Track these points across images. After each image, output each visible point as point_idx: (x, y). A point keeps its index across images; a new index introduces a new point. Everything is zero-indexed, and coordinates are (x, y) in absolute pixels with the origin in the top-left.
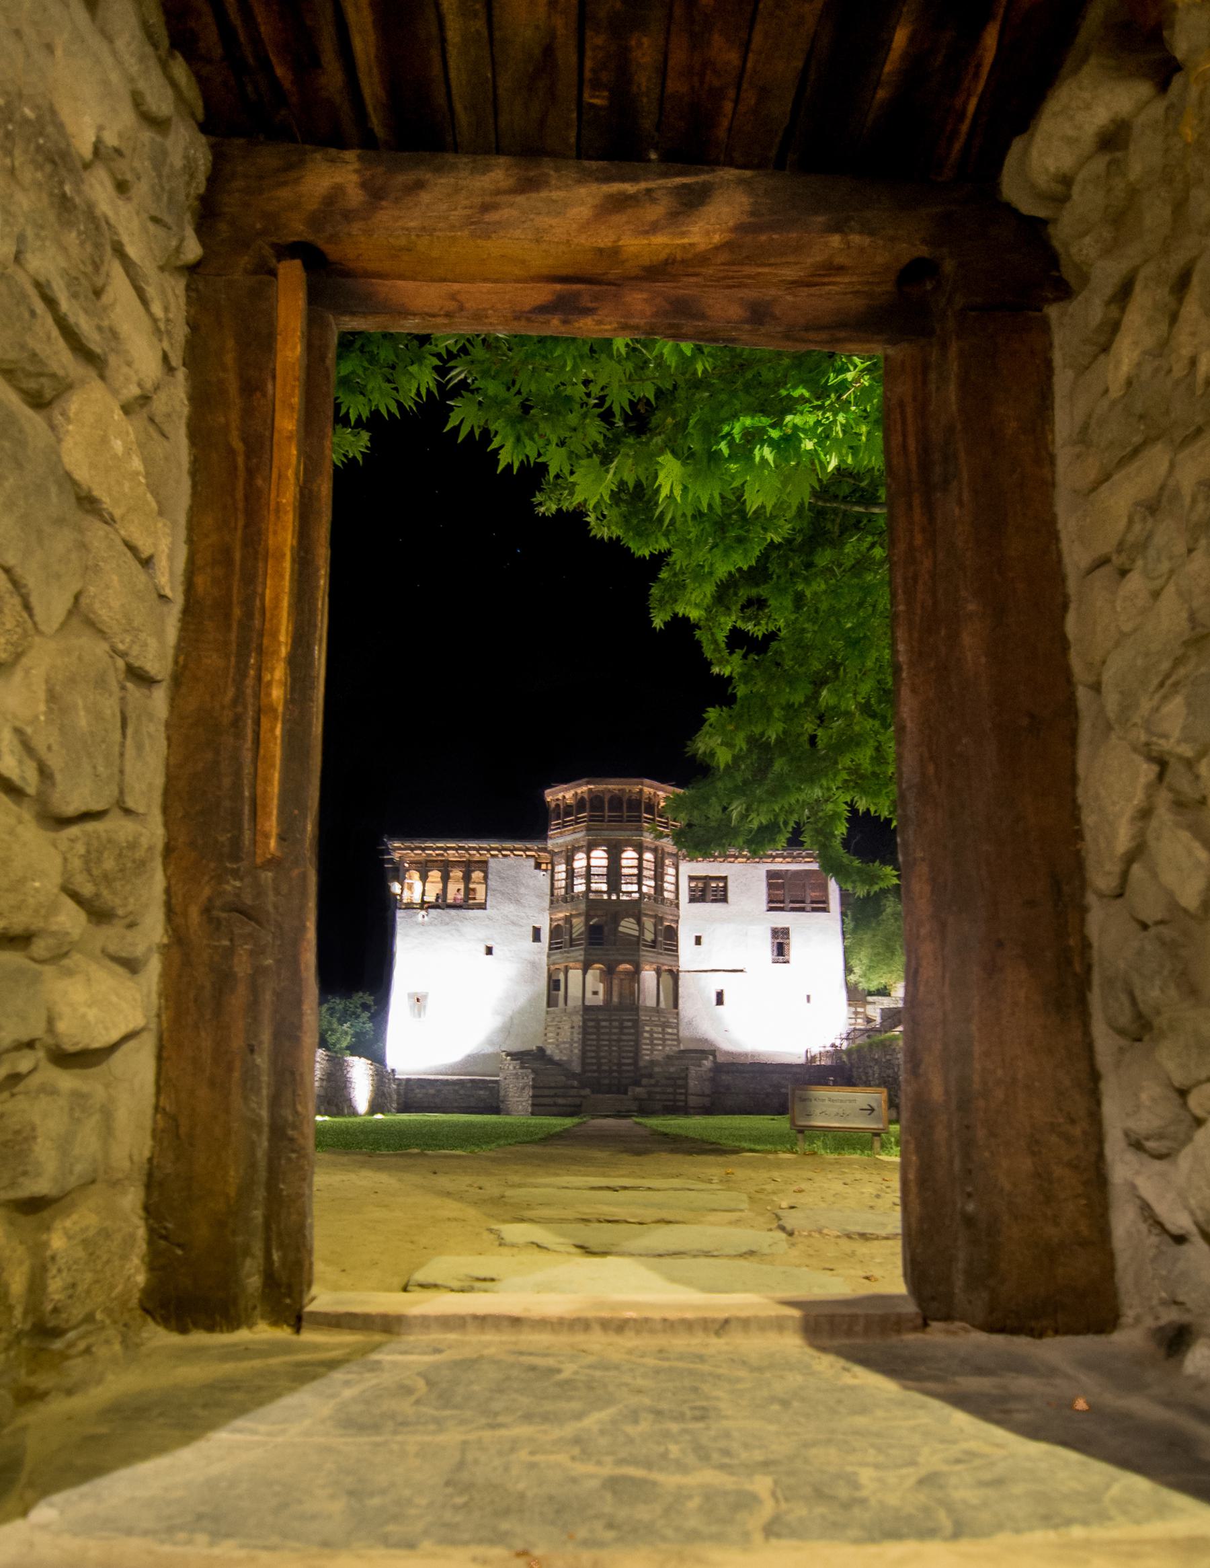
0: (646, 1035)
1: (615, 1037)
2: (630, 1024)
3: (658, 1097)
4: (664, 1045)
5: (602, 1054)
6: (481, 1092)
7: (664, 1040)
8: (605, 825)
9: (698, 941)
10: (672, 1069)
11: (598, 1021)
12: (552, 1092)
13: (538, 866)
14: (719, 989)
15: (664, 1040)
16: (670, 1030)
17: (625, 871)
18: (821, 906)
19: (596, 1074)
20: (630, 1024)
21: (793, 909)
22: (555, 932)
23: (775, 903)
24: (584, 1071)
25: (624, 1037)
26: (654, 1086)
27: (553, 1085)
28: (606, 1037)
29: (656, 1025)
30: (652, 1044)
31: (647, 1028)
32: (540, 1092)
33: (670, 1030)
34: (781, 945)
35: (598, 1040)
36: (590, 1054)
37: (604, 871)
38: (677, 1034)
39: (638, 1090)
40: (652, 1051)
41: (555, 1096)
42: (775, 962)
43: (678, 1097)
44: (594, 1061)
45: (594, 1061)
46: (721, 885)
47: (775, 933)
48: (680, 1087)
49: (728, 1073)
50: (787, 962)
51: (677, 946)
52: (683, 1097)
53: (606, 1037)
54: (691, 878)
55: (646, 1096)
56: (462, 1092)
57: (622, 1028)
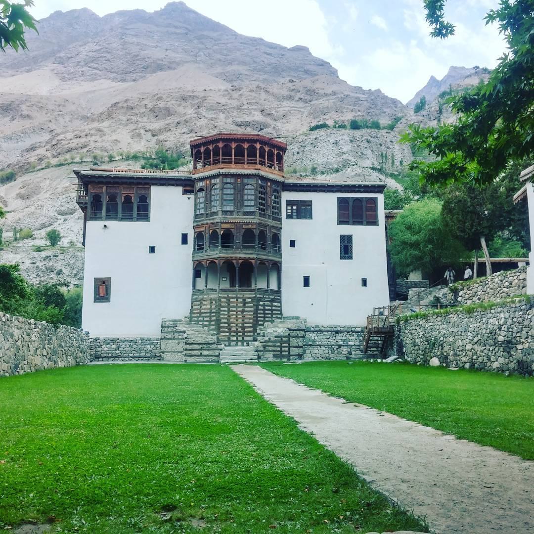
0: (260, 307)
1: (239, 309)
2: (250, 300)
3: (270, 349)
4: (272, 314)
5: (231, 320)
6: (149, 346)
7: (272, 310)
8: (233, 166)
9: (292, 244)
10: (279, 331)
11: (228, 299)
12: (199, 347)
13: (185, 192)
16: (276, 304)
17: (246, 197)
18: (375, 223)
19: (228, 334)
20: (250, 300)
21: (353, 224)
22: (199, 237)
23: (343, 220)
24: (219, 332)
25: (246, 309)
26: (266, 341)
27: (199, 342)
28: (235, 309)
30: (264, 314)
31: (261, 303)
32: (188, 347)
33: (276, 304)
34: (346, 248)
35: (229, 311)
36: (223, 320)
37: (232, 197)
38: (281, 307)
39: (256, 343)
40: (264, 317)
41: (201, 349)
42: (342, 258)
43: (283, 349)
44: (226, 325)
45: (226, 325)
47: (343, 238)
48: (285, 342)
49: (313, 332)
50: (351, 258)
51: (280, 247)
52: (286, 349)
54: (289, 203)
55: (262, 349)
56: (135, 346)
57: (245, 303)
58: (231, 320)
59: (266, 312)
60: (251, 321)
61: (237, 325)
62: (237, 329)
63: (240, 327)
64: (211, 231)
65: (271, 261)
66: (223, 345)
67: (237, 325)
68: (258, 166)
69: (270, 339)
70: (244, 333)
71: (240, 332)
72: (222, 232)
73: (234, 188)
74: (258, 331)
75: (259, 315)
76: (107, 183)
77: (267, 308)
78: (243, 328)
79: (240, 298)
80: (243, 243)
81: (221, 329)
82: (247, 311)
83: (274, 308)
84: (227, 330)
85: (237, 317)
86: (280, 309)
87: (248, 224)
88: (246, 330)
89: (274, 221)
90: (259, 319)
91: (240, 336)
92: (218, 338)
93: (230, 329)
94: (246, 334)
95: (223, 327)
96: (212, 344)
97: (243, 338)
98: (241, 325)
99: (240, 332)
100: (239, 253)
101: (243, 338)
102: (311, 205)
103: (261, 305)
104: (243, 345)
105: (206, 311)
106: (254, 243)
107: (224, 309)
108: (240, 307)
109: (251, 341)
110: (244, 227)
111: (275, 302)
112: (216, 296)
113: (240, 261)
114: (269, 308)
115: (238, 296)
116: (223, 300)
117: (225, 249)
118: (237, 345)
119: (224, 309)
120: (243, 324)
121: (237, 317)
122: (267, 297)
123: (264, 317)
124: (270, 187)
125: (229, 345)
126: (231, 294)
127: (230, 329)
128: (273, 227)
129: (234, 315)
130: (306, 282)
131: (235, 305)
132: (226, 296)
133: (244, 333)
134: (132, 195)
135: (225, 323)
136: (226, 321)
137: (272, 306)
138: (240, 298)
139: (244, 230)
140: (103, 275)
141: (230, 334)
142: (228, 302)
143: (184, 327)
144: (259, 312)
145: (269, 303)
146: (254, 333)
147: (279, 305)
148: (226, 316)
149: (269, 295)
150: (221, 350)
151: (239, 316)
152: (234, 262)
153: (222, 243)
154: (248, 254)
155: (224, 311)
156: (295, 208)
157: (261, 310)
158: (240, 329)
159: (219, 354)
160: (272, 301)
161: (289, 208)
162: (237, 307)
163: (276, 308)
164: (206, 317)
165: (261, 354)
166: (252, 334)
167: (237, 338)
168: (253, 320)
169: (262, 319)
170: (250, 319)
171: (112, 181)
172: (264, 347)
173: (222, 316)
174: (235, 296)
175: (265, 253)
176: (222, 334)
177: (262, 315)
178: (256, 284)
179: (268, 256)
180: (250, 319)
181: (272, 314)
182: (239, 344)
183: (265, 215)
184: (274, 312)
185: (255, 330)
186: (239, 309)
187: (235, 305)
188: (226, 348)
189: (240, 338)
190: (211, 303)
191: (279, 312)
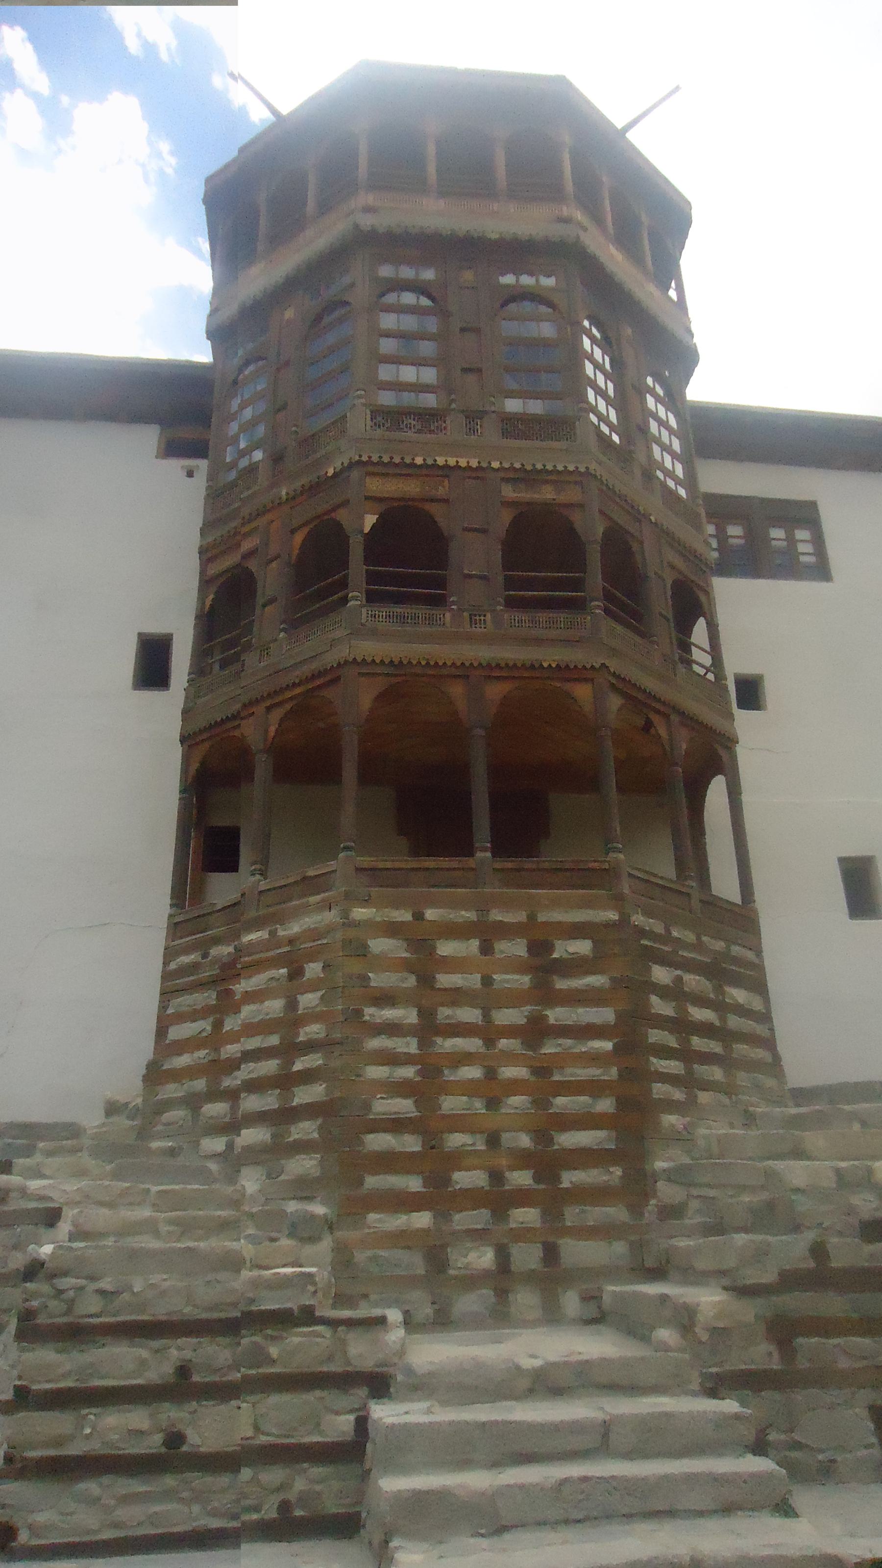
2: (582, 947)
5: (450, 1104)
16: (738, 995)
19: (422, 1220)
20: (582, 947)
22: (227, 605)
25: (556, 1015)
26: (790, 1281)
28: (469, 1015)
30: (686, 1055)
31: (661, 974)
33: (738, 995)
35: (429, 1029)
38: (766, 1017)
40: (689, 1082)
44: (411, 1143)
45: (411, 1143)
46: (802, 534)
53: (469, 1015)
57: (543, 965)
58: (450, 1104)
59: (697, 1042)
60: (606, 1105)
61: (493, 1141)
62: (496, 1177)
63: (524, 1159)
64: (299, 538)
66: (395, 1335)
67: (493, 1141)
69: (818, 1251)
70: (553, 1201)
71: (522, 1198)
72: (370, 520)
73: (441, 310)
74: (668, 1193)
78: (547, 1164)
80: (510, 583)
81: (372, 1182)
82: (563, 1031)
84: (414, 1184)
85: (491, 1074)
88: (569, 1179)
90: (659, 1090)
91: (523, 1234)
92: (343, 1260)
93: (438, 1181)
94: (572, 1215)
95: (388, 1162)
96: (283, 1319)
97: (551, 1253)
98: (525, 1141)
99: (522, 1198)
101: (551, 1253)
103: (665, 992)
104: (552, 1316)
105: (253, 1043)
106: (577, 585)
107: (389, 1014)
108: (514, 999)
109: (610, 1273)
110: (508, 492)
111: (738, 981)
112: (331, 917)
113: (495, 691)
115: (496, 915)
116: (379, 945)
117: (383, 611)
118: (500, 1317)
119: (389, 1014)
120: (542, 1136)
121: (491, 1074)
122: (690, 937)
123: (689, 1082)
125: (442, 1321)
126: (434, 904)
127: (438, 1181)
129: (466, 1058)
131: (474, 981)
132: (404, 916)
133: (553, 1201)
135: (396, 1125)
136: (405, 1106)
137: (721, 1007)
141: (442, 1216)
142: (424, 964)
143: (81, 1173)
146: (636, 1209)
148: (408, 1072)
150: (379, 1384)
151: (509, 1072)
152: (457, 690)
153: (372, 578)
154: (539, 642)
155: (393, 1029)
156: (735, 531)
157: (661, 1022)
158: (522, 1178)
159: (362, 1423)
162: (488, 997)
164: (254, 1086)
166: (617, 1213)
167: (503, 1254)
168: (622, 1103)
170: (594, 1088)
172: (783, 1331)
173: (376, 1072)
174: (470, 915)
176: (380, 1221)
180: (594, 1088)
182: (525, 1299)
184: (741, 1049)
185: (637, 1187)
186: (507, 1016)
187: (474, 981)
188: (433, 1353)
189: (527, 1257)
190: (296, 973)
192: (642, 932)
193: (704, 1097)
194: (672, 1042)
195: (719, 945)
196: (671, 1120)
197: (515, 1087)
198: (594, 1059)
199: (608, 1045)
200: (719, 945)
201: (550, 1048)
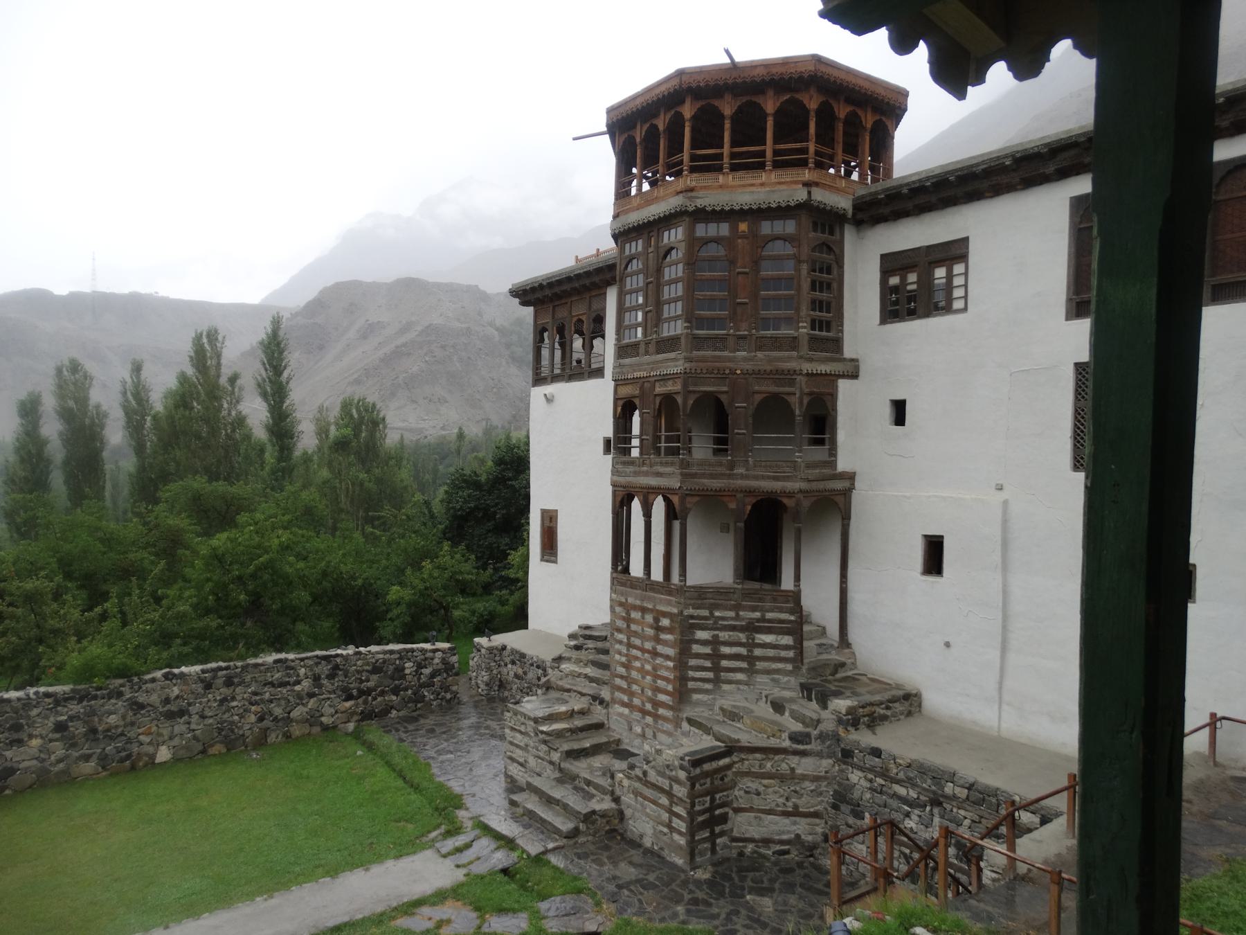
0: (696, 648)
2: (665, 622)
4: (751, 671)
5: (634, 674)
7: (751, 659)
9: (899, 411)
14: (933, 531)
15: (751, 659)
16: (769, 638)
19: (626, 711)
20: (665, 622)
25: (660, 648)
29: (733, 628)
30: (716, 669)
31: (702, 635)
40: (717, 681)
46: (958, 268)
54: (892, 264)
59: (724, 663)
65: (749, 492)
68: (689, 180)
75: (691, 673)
76: (551, 300)
77: (726, 650)
79: (651, 611)
82: (661, 655)
83: (758, 652)
86: (791, 654)
87: (665, 379)
89: (760, 354)
90: (691, 685)
91: (648, 725)
100: (646, 474)
102: (963, 258)
103: (704, 643)
110: (659, 389)
111: (769, 631)
114: (743, 651)
122: (732, 614)
124: (753, 235)
128: (759, 375)
130: (933, 555)
134: (584, 318)
138: (651, 611)
139: (658, 400)
140: (549, 506)
142: (628, 620)
144: (692, 662)
145: (742, 637)
147: (787, 640)
149: (737, 608)
151: (648, 667)
155: (620, 642)
157: (698, 656)
158: (649, 707)
160: (752, 628)
161: (894, 281)
163: (771, 653)
165: (628, 812)
169: (708, 686)
171: (548, 292)
175: (720, 470)
177: (710, 675)
178: (683, 573)
179: (730, 476)
181: (751, 671)
183: (723, 339)
184: (760, 665)
189: (649, 733)
191: (789, 667)
192: (692, 617)
193: (725, 687)
194: (708, 664)
195: (757, 615)
196: (695, 697)
197: (648, 673)
198: (667, 668)
199: (671, 664)
200: (757, 615)
201: (659, 661)
